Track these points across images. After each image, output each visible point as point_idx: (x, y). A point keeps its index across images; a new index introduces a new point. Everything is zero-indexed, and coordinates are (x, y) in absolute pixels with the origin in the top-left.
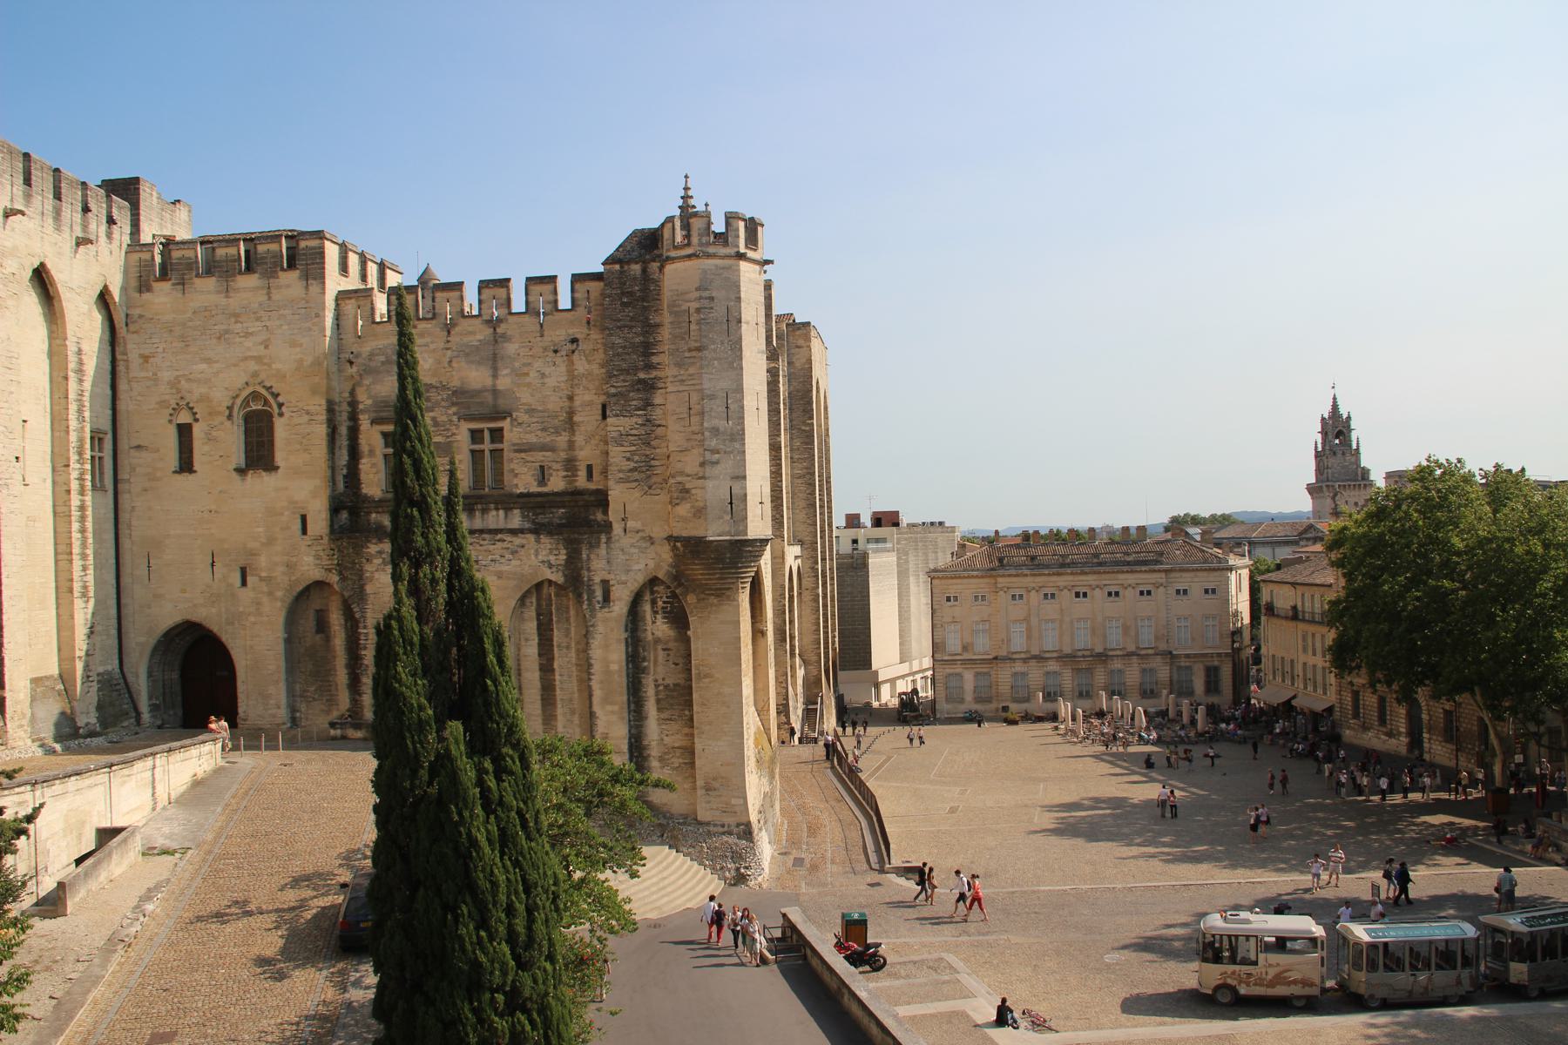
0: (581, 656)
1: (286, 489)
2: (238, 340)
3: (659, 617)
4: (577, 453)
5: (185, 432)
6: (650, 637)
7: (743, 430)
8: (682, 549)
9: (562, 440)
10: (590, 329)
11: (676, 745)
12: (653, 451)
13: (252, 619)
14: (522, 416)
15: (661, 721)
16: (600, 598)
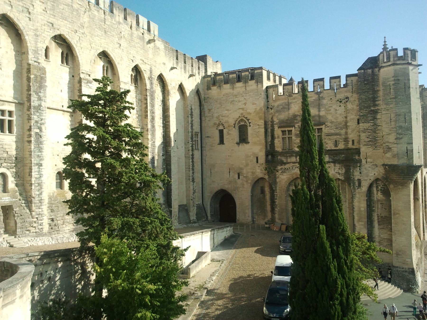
0: (350, 205)
1: (252, 149)
2: (236, 103)
3: (379, 192)
4: (348, 136)
5: (221, 132)
6: (376, 199)
7: (411, 126)
8: (388, 169)
9: (343, 132)
10: (353, 93)
11: (385, 238)
12: (377, 134)
13: (241, 189)
15: (380, 229)
16: (357, 185)
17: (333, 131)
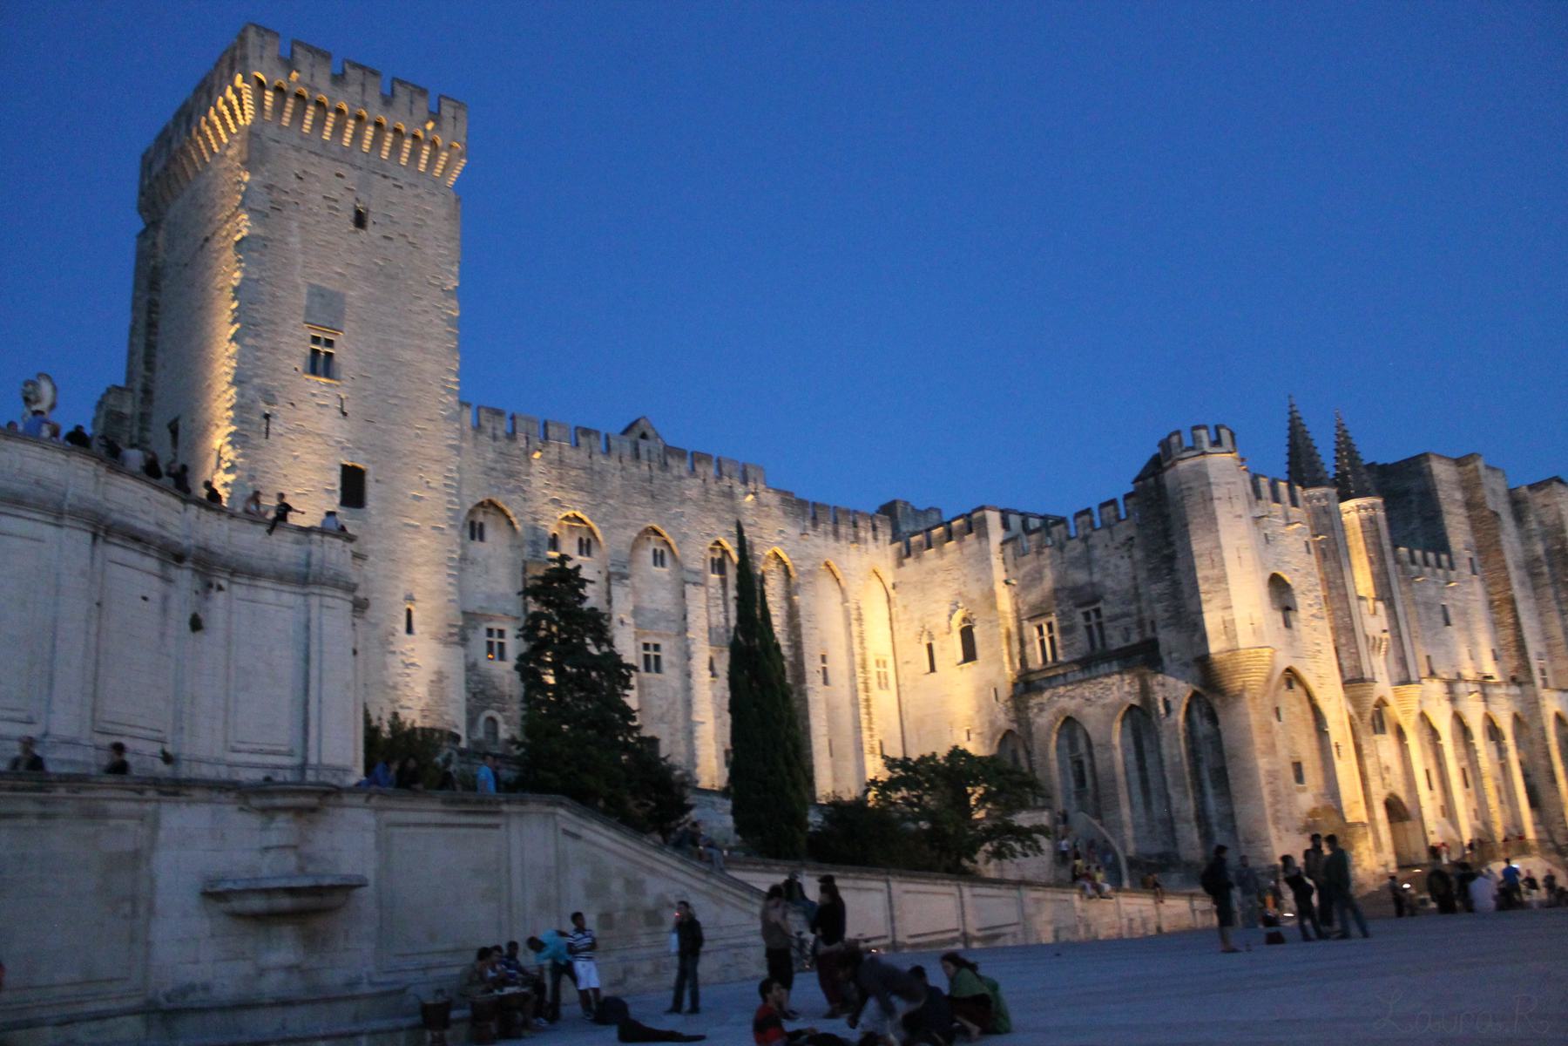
3: (1205, 722)
9: (1133, 608)
14: (1109, 597)
17: (1117, 610)
